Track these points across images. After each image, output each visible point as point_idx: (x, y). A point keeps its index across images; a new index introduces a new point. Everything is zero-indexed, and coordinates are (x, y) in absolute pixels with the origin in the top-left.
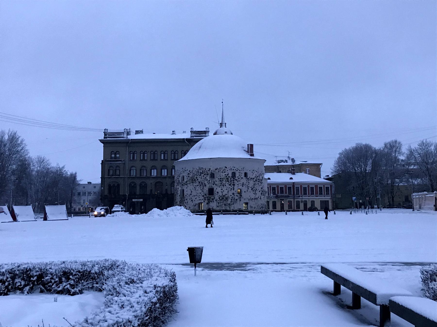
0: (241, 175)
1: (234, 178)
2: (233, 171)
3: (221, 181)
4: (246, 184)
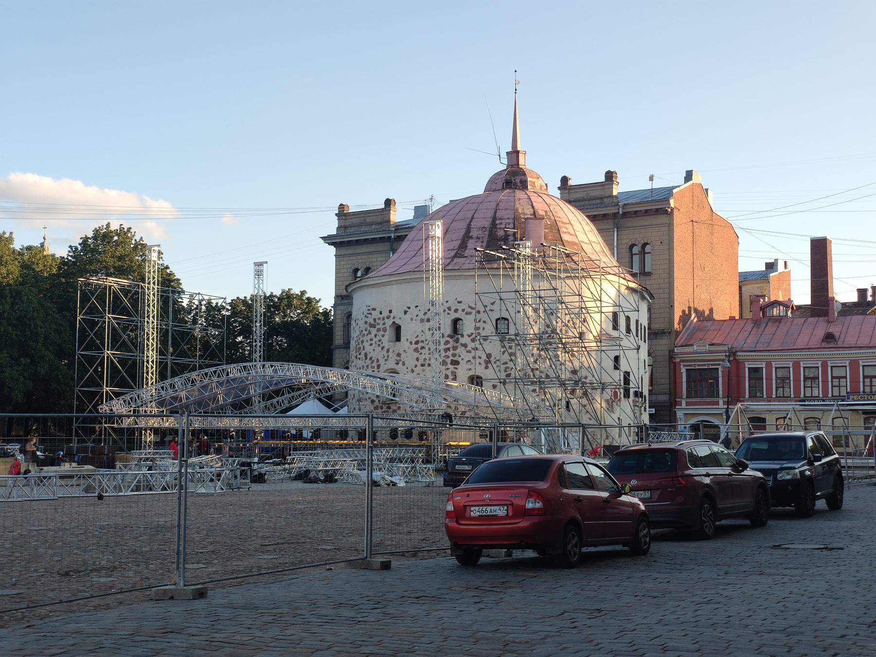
0: (484, 329)
1: (457, 341)
2: (454, 316)
3: (416, 350)
4: (498, 360)
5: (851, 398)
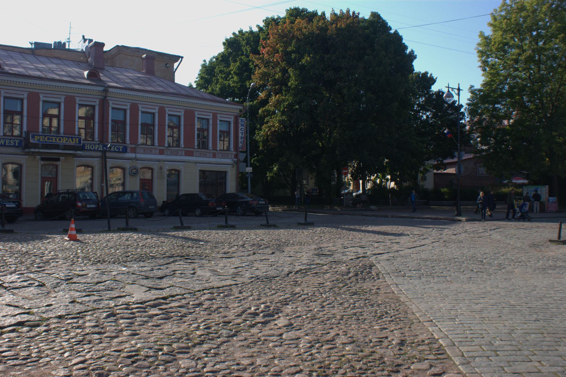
5: (36, 139)
